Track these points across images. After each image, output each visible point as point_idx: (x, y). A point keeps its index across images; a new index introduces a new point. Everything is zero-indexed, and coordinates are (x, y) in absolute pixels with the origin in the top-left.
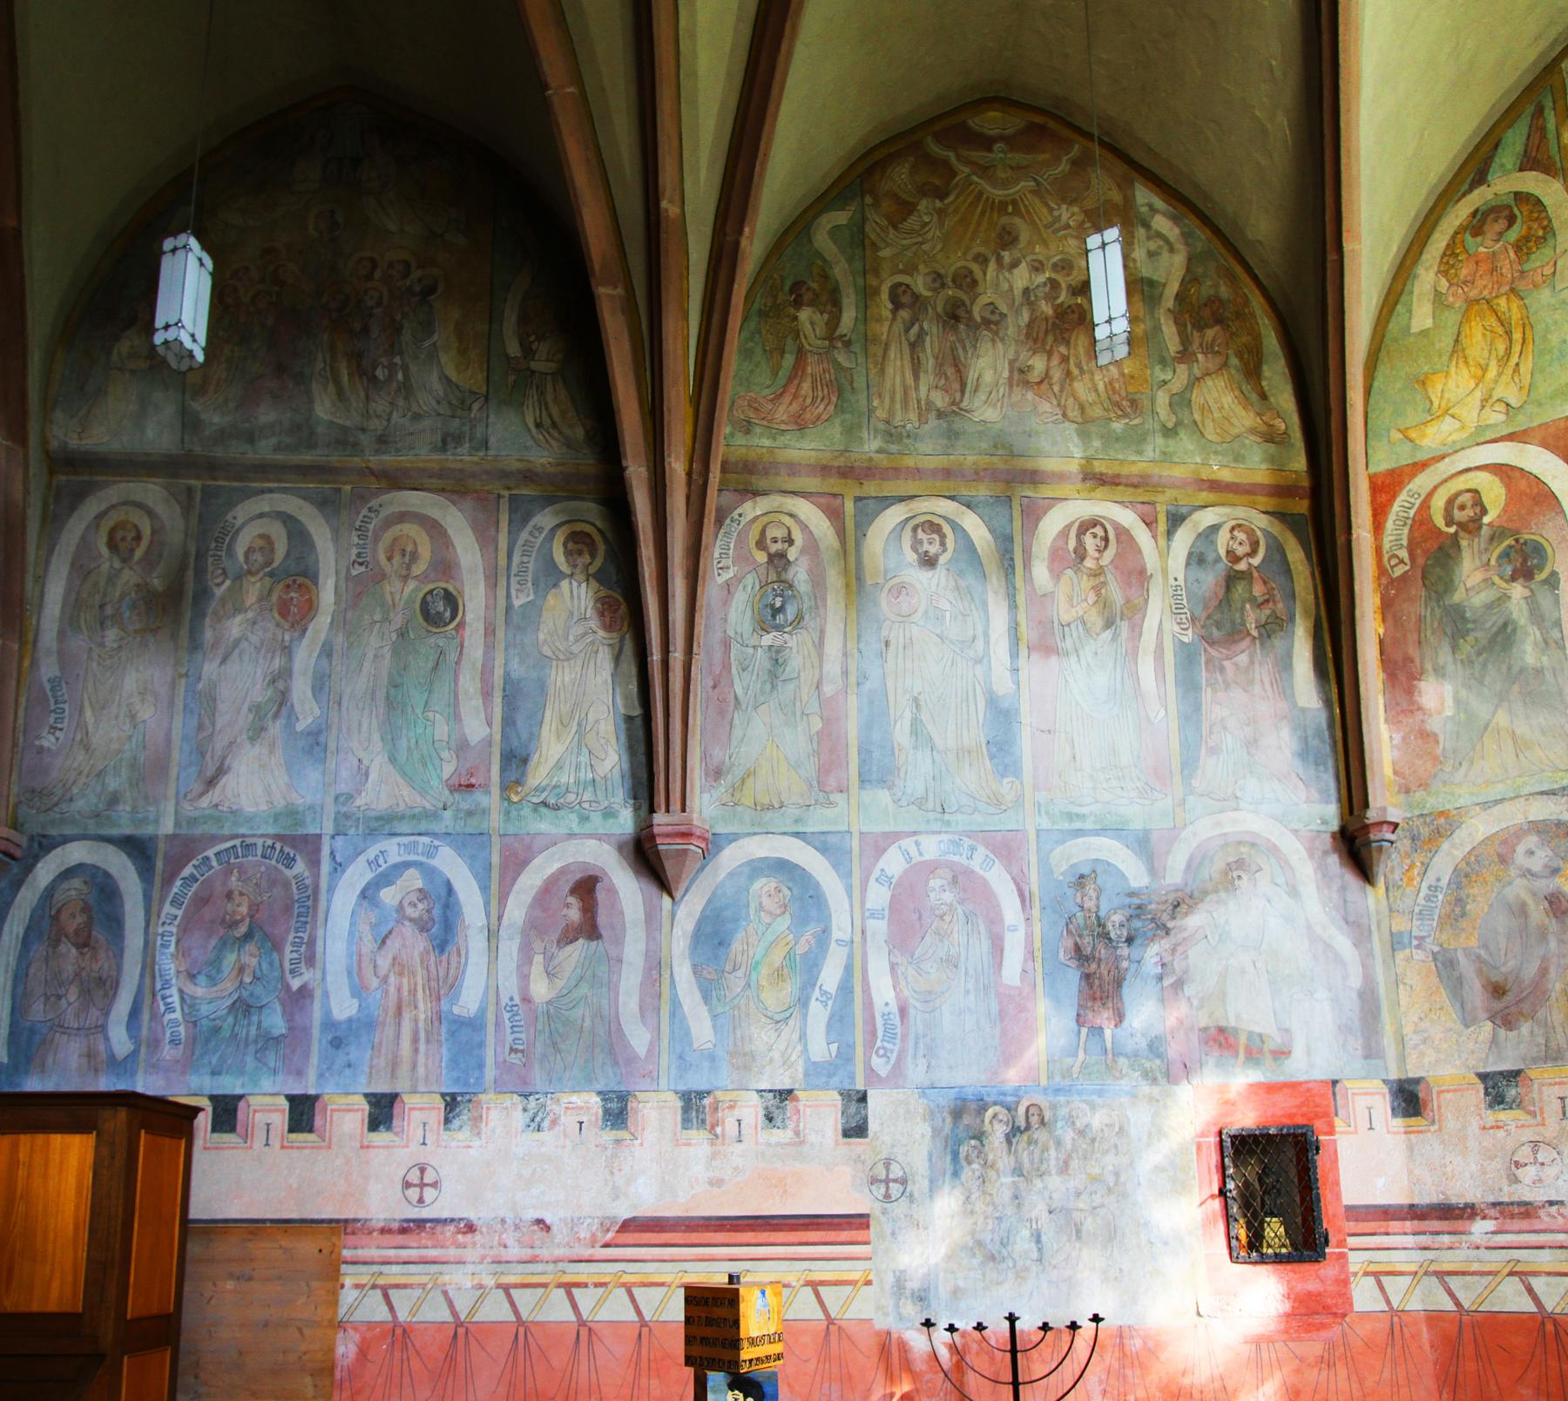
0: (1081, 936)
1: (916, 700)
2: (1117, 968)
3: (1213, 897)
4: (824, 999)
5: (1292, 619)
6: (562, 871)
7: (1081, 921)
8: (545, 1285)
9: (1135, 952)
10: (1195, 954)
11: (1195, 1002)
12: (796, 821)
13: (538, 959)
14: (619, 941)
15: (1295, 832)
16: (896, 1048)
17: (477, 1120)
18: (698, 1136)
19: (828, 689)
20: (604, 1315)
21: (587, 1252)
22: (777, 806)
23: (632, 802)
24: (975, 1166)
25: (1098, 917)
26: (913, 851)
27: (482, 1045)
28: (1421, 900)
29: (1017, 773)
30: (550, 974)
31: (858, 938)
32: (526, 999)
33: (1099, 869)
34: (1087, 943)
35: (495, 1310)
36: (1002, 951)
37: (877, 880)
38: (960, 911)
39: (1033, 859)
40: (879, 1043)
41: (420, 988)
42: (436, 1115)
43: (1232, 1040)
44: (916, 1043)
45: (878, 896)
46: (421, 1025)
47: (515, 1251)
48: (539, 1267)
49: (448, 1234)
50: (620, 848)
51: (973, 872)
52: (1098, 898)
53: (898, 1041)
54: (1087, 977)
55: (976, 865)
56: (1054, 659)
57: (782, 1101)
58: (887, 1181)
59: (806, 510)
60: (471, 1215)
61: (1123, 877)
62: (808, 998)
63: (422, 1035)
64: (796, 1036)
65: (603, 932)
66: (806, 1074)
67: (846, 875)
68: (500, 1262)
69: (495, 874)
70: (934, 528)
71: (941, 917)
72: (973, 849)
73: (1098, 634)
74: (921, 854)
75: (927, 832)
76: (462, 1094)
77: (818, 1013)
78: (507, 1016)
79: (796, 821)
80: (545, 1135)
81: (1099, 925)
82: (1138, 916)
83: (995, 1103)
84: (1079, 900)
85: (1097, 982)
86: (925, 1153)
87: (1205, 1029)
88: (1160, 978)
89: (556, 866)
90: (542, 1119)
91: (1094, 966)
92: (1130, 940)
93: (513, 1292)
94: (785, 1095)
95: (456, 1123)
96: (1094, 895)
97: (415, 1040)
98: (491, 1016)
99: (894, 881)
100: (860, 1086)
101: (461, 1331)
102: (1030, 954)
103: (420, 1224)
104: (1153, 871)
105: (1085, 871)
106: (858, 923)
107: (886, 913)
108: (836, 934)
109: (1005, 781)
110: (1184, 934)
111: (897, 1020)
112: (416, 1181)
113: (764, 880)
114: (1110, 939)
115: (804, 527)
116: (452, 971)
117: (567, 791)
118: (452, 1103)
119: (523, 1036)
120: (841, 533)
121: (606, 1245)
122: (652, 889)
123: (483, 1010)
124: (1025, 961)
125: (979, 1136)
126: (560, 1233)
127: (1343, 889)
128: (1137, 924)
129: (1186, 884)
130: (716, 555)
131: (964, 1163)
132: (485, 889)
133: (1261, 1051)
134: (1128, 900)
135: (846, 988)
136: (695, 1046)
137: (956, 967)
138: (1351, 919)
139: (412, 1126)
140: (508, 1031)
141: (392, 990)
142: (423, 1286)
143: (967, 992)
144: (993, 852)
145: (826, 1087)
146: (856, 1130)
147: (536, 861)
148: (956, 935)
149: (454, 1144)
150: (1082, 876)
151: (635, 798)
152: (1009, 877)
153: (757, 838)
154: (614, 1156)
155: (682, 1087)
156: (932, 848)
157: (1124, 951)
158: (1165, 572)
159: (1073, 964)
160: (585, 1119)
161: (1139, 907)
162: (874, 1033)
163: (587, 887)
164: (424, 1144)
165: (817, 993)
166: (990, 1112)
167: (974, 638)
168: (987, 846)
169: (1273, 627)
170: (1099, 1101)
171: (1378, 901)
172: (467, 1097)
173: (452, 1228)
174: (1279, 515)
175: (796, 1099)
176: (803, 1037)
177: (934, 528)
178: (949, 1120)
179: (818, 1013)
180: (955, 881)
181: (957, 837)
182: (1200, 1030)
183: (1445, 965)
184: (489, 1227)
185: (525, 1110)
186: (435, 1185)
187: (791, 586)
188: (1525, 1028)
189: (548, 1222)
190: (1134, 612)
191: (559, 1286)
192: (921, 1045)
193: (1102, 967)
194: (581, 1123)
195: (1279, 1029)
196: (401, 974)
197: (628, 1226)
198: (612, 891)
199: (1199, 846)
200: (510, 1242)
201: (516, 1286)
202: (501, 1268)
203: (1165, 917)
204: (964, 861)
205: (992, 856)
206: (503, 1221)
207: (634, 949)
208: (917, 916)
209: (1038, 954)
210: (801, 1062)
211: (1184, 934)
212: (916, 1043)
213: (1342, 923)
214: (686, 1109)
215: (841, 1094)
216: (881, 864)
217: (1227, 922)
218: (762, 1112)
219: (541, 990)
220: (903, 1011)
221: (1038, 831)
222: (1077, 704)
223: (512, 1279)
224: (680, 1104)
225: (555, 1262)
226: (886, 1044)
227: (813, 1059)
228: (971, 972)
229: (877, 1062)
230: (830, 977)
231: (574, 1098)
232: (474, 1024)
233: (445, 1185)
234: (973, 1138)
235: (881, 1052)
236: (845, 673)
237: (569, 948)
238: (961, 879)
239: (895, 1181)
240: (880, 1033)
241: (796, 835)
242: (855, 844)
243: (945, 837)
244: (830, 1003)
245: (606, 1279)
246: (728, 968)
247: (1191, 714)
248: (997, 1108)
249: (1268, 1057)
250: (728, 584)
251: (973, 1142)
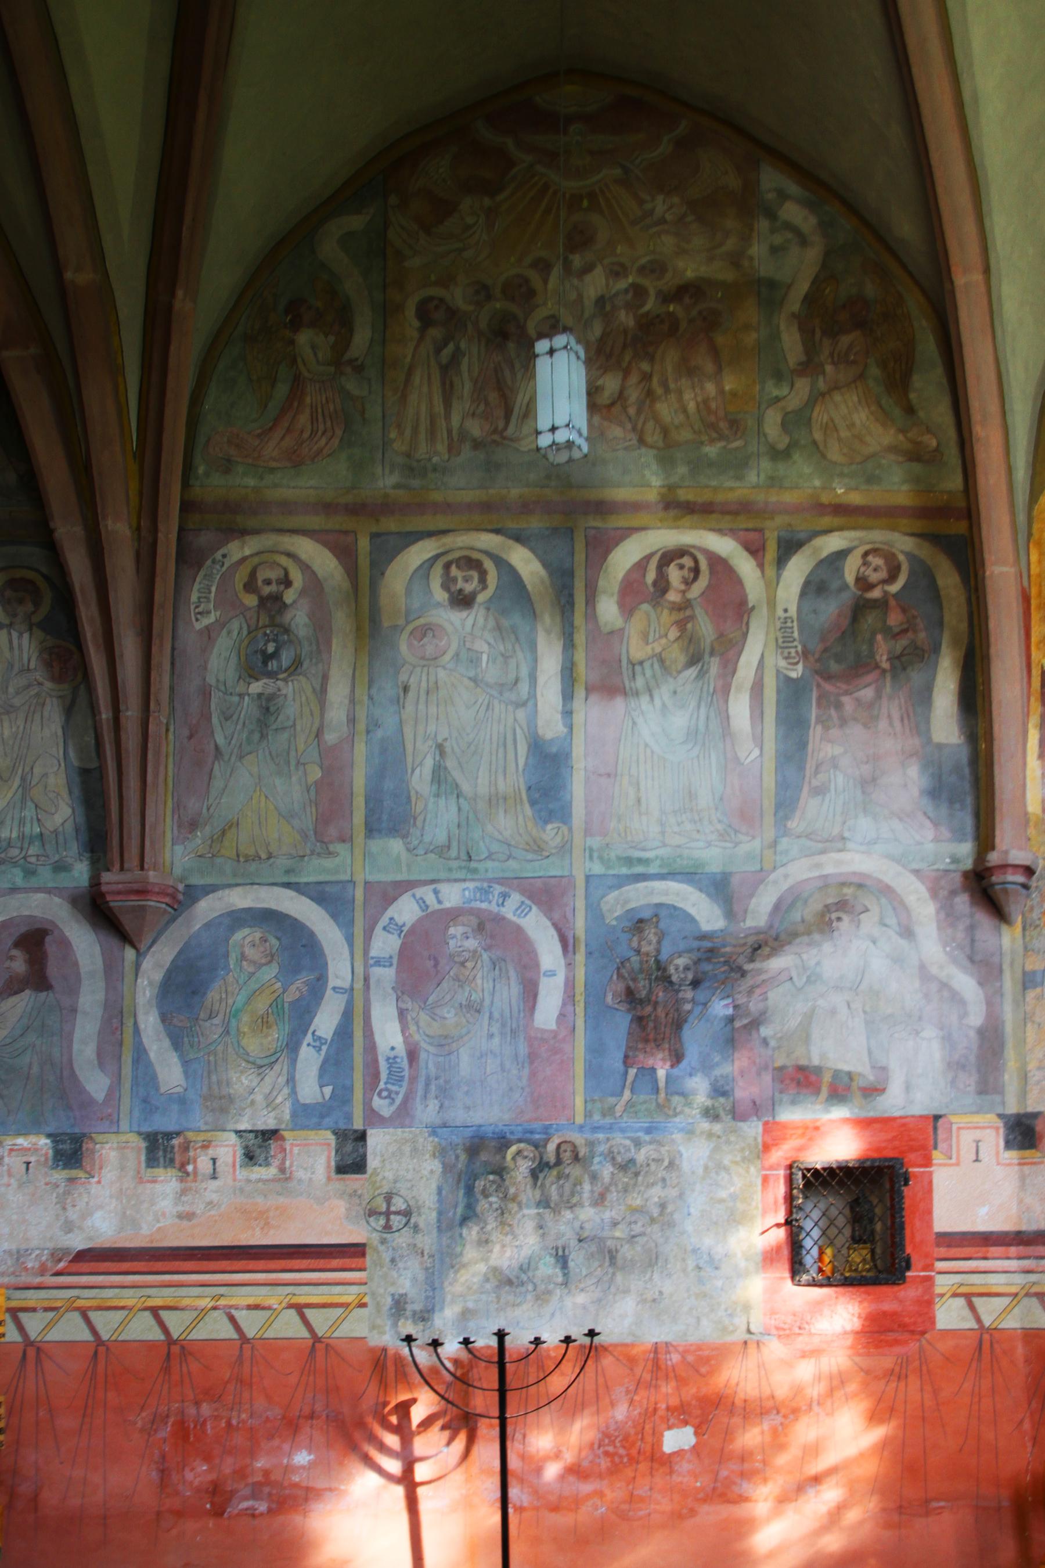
0: (634, 980)
1: (440, 748)
2: (677, 1010)
3: (805, 939)
4: (317, 1044)
7: (636, 966)
9: (701, 995)
10: (775, 996)
11: (773, 1043)
12: (288, 872)
16: (403, 1091)
19: (330, 738)
22: (264, 856)
24: (493, 1199)
25: (658, 962)
26: (430, 899)
29: (563, 815)
31: (359, 985)
33: (663, 913)
34: (642, 987)
36: (535, 996)
37: (384, 928)
38: (485, 956)
39: (580, 904)
40: (382, 1085)
43: (813, 1078)
44: (427, 1084)
51: (504, 918)
52: (659, 942)
53: (405, 1084)
54: (640, 1021)
55: (508, 911)
56: (619, 702)
58: (388, 1214)
59: (307, 548)
61: (692, 920)
70: (471, 563)
71: (463, 964)
72: (505, 896)
73: (679, 672)
74: (440, 902)
75: (448, 880)
77: (309, 1059)
79: (288, 872)
81: (659, 969)
82: (708, 960)
83: (520, 1141)
84: (635, 944)
85: (651, 1024)
86: (434, 1186)
87: (781, 1069)
88: (731, 1020)
91: (648, 1009)
92: (695, 984)
96: (654, 940)
99: (405, 929)
100: (358, 1125)
102: (569, 996)
104: (730, 914)
105: (646, 914)
107: (395, 961)
108: (332, 983)
109: (549, 827)
110: (764, 977)
111: (405, 1064)
114: (671, 983)
115: (306, 568)
120: (352, 571)
124: (564, 1004)
125: (500, 1171)
127: (972, 928)
128: (706, 967)
129: (771, 927)
130: (194, 597)
131: (480, 1197)
133: (848, 1088)
134: (696, 944)
135: (344, 1033)
136: (162, 1090)
137: (478, 1011)
138: (978, 958)
143: (491, 1036)
144: (530, 898)
148: (479, 981)
150: (641, 921)
152: (548, 923)
153: (239, 889)
156: (453, 896)
157: (689, 994)
159: (623, 1007)
161: (711, 950)
162: (376, 1076)
165: (309, 1038)
166: (513, 1149)
167: (517, 681)
168: (523, 892)
170: (647, 1138)
171: (1013, 940)
176: (291, 1080)
177: (471, 563)
178: (463, 1157)
179: (309, 1059)
180: (480, 928)
181: (485, 885)
182: (775, 1069)
187: (287, 631)
192: (433, 1088)
193: (659, 1010)
195: (873, 1067)
199: (791, 888)
203: (741, 960)
204: (494, 908)
205: (528, 902)
208: (432, 963)
209: (580, 998)
211: (764, 977)
212: (427, 1084)
213: (966, 963)
215: (335, 1133)
216: (391, 912)
217: (818, 964)
220: (412, 1055)
222: (646, 745)
226: (389, 1086)
227: (302, 1101)
228: (496, 1015)
229: (377, 1103)
234: (492, 1173)
235: (385, 1094)
236: (352, 720)
239: (398, 1213)
240: (384, 1076)
241: (287, 885)
242: (359, 894)
243: (471, 885)
244: (324, 1048)
246: (202, 1015)
248: (522, 1145)
249: (858, 1094)
250: (208, 628)
251: (491, 1177)
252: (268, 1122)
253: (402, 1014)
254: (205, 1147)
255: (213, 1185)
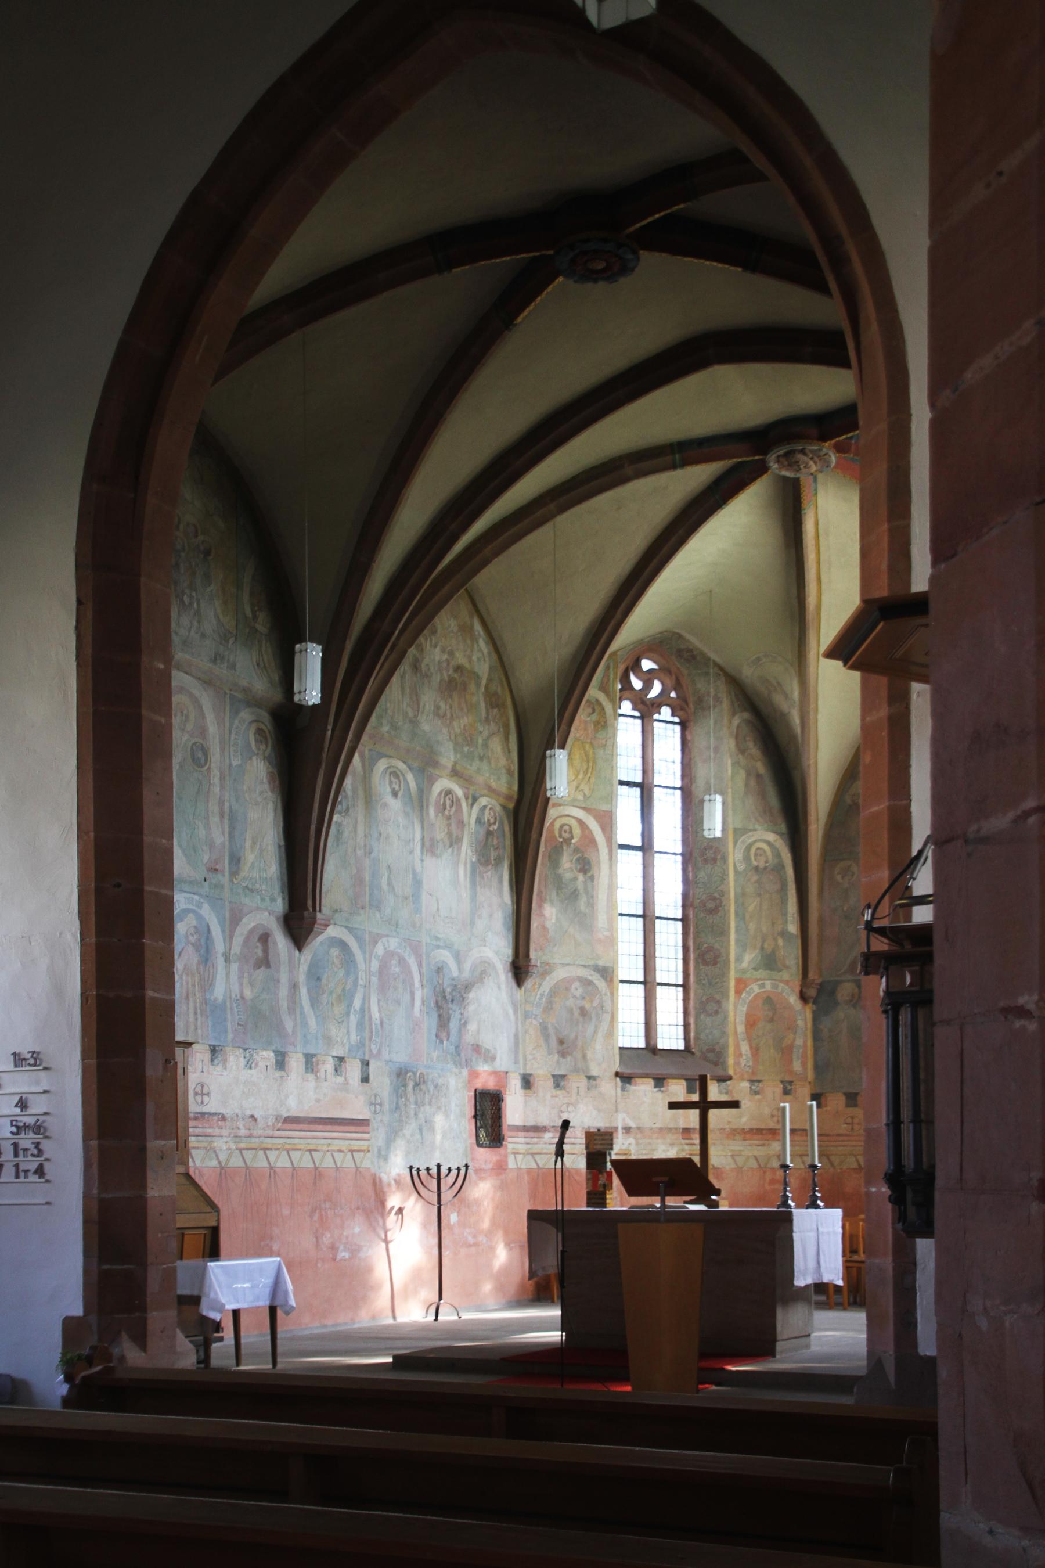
5: (504, 859)
6: (255, 927)
8: (255, 1149)
13: (246, 975)
14: (278, 971)
15: (500, 959)
17: (225, 1061)
18: (311, 1077)
20: (279, 1164)
21: (270, 1132)
23: (281, 894)
27: (225, 1020)
28: (537, 999)
30: (252, 984)
31: (367, 985)
32: (242, 998)
35: (236, 1162)
41: (196, 984)
42: (208, 1056)
45: (375, 965)
46: (198, 1005)
47: (243, 1132)
48: (253, 1140)
49: (215, 1121)
50: (278, 919)
54: (440, 1016)
57: (341, 1062)
60: (223, 1111)
62: (350, 1012)
63: (199, 1011)
64: (345, 1031)
65: (272, 966)
66: (349, 1050)
67: (364, 952)
68: (237, 1137)
69: (228, 923)
76: (219, 1046)
77: (353, 1019)
78: (235, 1005)
80: (253, 1071)
89: (252, 924)
90: (252, 1063)
93: (243, 1152)
94: (341, 1059)
95: (216, 1062)
97: (196, 1013)
98: (228, 1004)
100: (367, 1058)
101: (223, 1171)
103: (203, 1114)
106: (368, 977)
112: (200, 1092)
113: (334, 949)
116: (211, 976)
117: (256, 883)
118: (214, 1050)
119: (242, 1017)
121: (278, 1130)
122: (292, 945)
123: (224, 1002)
126: (261, 1123)
132: (223, 931)
135: (362, 1010)
139: (197, 1062)
140: (236, 1014)
141: (184, 983)
142: (206, 1148)
145: (355, 1058)
146: (365, 1079)
147: (244, 920)
149: (215, 1073)
150: (439, 968)
151: (283, 893)
154: (280, 1085)
155: (305, 1052)
158: (469, 824)
160: (268, 1064)
163: (265, 938)
164: (203, 1072)
169: (499, 861)
172: (220, 1048)
173: (215, 1118)
174: (504, 807)
175: (345, 1062)
179: (353, 1019)
183: (544, 1029)
184: (232, 1119)
185: (245, 1057)
186: (208, 1094)
188: (569, 1058)
189: (256, 1117)
190: (459, 840)
191: (261, 1149)
194: (267, 1066)
196: (187, 975)
197: (288, 1120)
198: (275, 943)
200: (241, 1126)
201: (244, 1149)
202: (237, 1140)
206: (237, 1115)
207: (284, 978)
210: (347, 1044)
214: (307, 1063)
218: (333, 1068)
219: (248, 993)
221: (426, 943)
223: (242, 1145)
224: (304, 1060)
225: (259, 1137)
230: (357, 1003)
231: (264, 1053)
232: (223, 1008)
233: (212, 1095)
237: (258, 971)
238: (402, 962)
245: (279, 1146)
247: (474, 897)
252: (341, 1054)
253: (379, 1001)
254: (323, 1064)
255: (326, 1084)
